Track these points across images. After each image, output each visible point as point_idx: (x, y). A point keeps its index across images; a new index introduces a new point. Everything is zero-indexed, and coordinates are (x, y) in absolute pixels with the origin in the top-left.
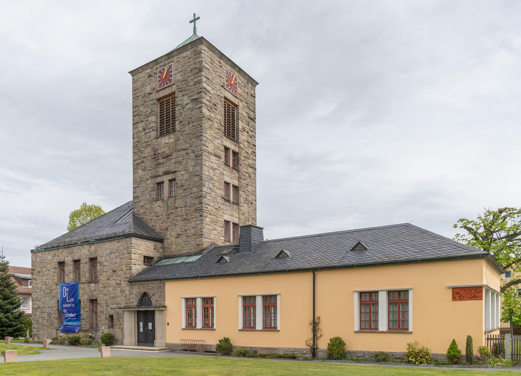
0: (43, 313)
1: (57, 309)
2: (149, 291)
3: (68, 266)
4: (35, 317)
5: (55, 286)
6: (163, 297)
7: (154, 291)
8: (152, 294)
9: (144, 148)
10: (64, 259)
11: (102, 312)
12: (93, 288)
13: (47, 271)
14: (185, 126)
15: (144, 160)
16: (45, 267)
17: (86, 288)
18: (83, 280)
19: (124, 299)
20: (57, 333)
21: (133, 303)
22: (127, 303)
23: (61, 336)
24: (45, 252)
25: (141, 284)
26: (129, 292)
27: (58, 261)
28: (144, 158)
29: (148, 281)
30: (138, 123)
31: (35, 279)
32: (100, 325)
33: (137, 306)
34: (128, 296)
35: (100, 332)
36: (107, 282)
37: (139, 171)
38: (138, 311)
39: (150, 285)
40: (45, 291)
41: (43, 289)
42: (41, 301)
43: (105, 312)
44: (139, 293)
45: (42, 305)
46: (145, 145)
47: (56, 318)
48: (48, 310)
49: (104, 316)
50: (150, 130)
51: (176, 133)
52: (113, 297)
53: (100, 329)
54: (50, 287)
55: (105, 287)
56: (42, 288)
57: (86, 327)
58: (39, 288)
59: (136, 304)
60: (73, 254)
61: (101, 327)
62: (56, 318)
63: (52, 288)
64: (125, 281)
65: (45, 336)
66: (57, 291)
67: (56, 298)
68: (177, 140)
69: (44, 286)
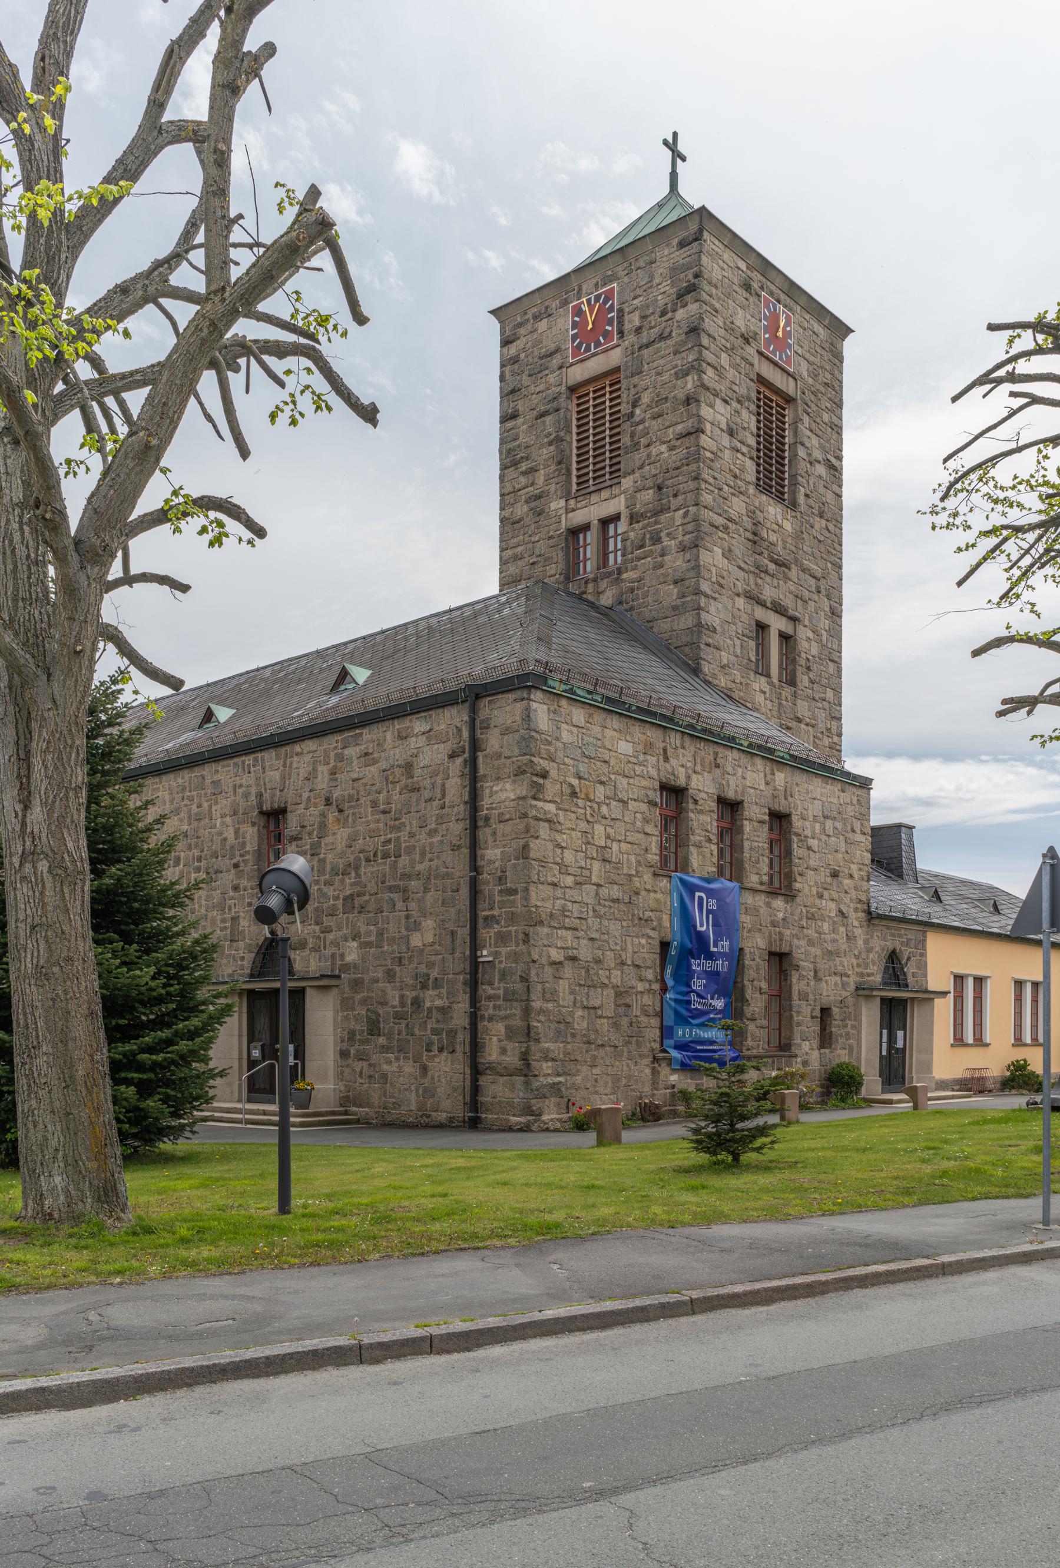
0: (595, 987)
3: (701, 812)
4: (550, 1006)
5: (648, 877)
6: (923, 966)
10: (688, 777)
11: (804, 997)
12: (781, 915)
13: (614, 803)
16: (602, 783)
17: (762, 911)
18: (753, 880)
19: (855, 962)
20: (655, 1072)
21: (872, 974)
22: (862, 975)
23: (673, 1086)
24: (603, 715)
25: (888, 928)
27: (664, 780)
31: (549, 821)
32: (797, 1040)
33: (884, 984)
34: (864, 955)
36: (817, 901)
40: (604, 892)
41: (594, 879)
42: (581, 934)
43: (811, 997)
45: (585, 952)
48: (616, 976)
52: (830, 953)
55: (811, 917)
56: (587, 873)
57: (758, 1046)
58: (571, 870)
60: (718, 771)
61: (800, 1045)
64: (856, 910)
65: (601, 1090)
66: (657, 900)
67: (654, 929)
69: (596, 866)
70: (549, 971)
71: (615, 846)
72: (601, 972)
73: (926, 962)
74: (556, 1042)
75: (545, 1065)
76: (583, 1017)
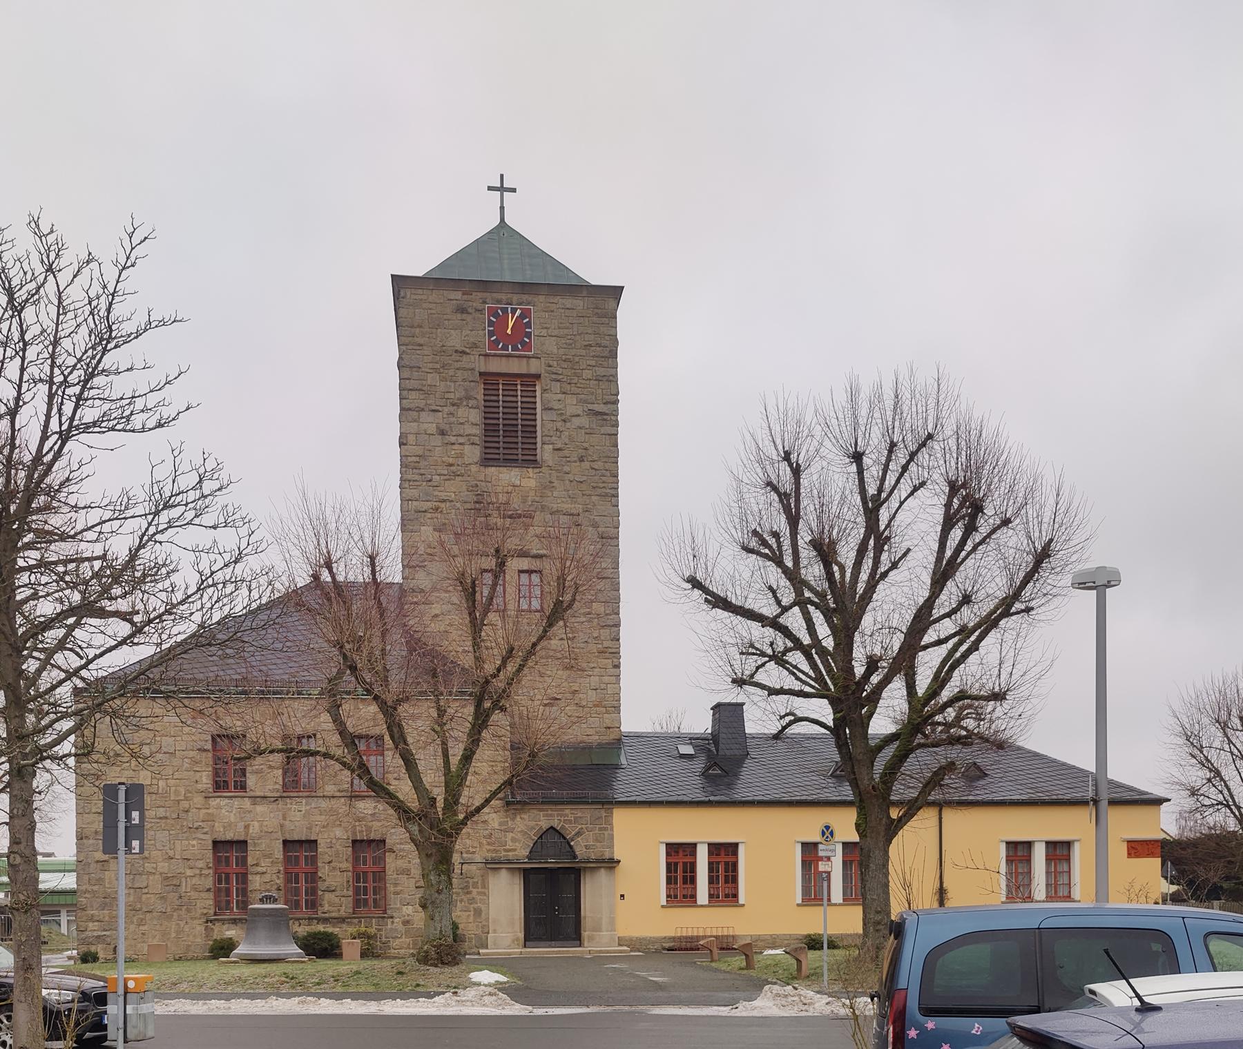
1: (211, 865)
2: (567, 826)
4: (95, 888)
5: (198, 800)
7: (580, 827)
8: (573, 833)
9: (442, 477)
11: (407, 872)
14: (569, 462)
15: (443, 505)
21: (515, 850)
26: (500, 824)
28: (444, 501)
29: (562, 803)
30: (423, 410)
33: (529, 857)
35: (396, 920)
37: (422, 528)
38: (525, 870)
39: (567, 812)
44: (533, 828)
46: (446, 472)
47: (209, 890)
48: (163, 866)
49: (414, 880)
50: (461, 440)
51: (543, 469)
53: (394, 914)
54: (178, 801)
57: (339, 911)
59: (526, 852)
62: (209, 890)
63: (185, 805)
66: (209, 814)
68: (547, 486)
70: (93, 866)
71: (161, 783)
72: (146, 865)
73: (612, 837)
74: (103, 910)
75: (91, 924)
76: (129, 894)
